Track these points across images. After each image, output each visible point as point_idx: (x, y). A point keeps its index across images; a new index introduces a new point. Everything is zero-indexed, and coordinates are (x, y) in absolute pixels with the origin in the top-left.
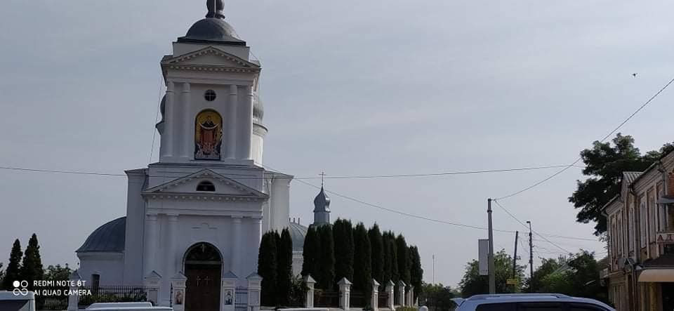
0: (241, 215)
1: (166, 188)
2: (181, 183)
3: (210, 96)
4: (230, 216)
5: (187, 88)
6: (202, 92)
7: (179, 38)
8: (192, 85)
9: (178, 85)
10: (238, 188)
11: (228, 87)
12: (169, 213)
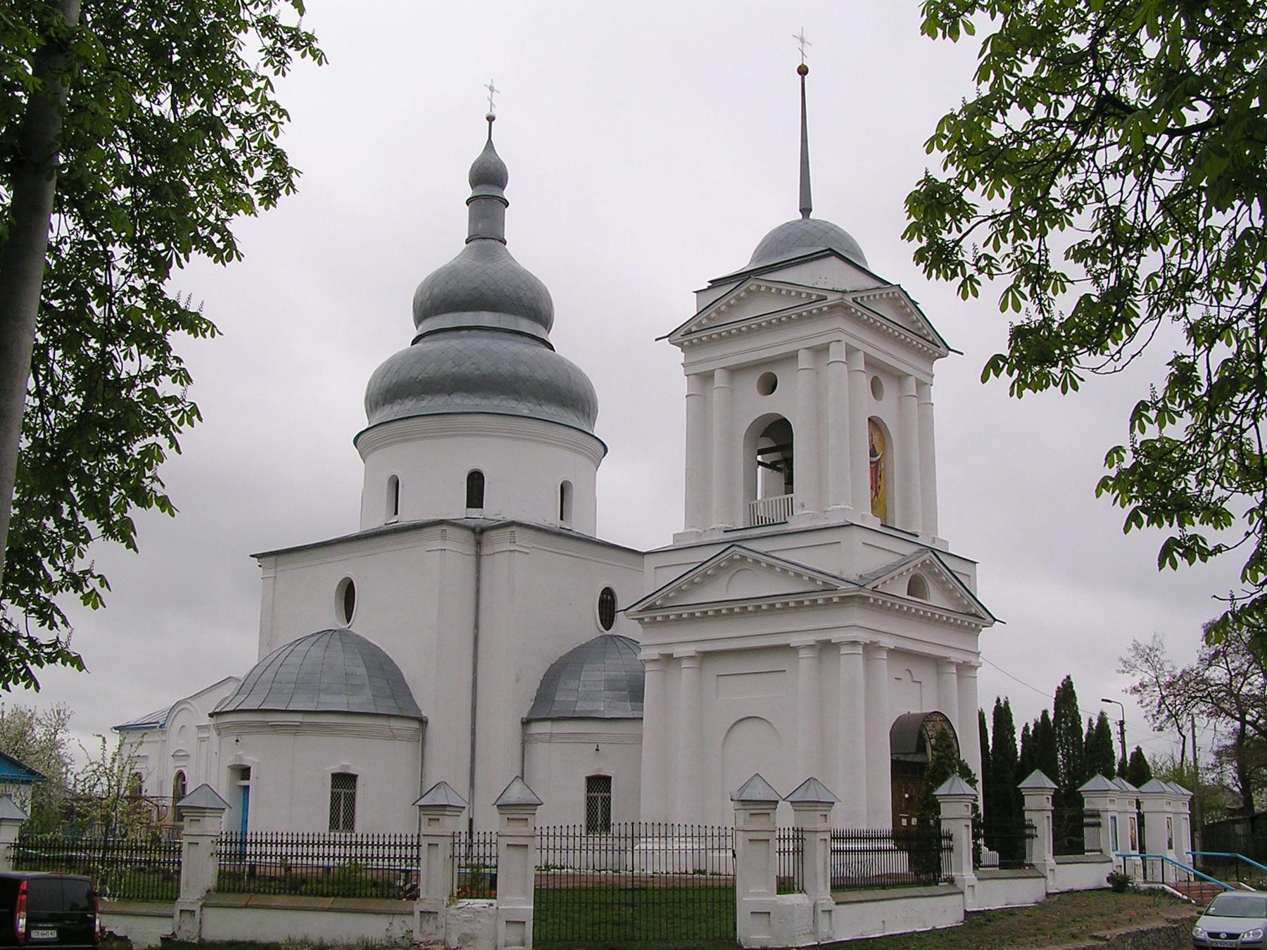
0: (810, 639)
1: (666, 597)
2: (692, 583)
3: (769, 385)
4: (786, 648)
5: (720, 379)
6: (751, 383)
7: (710, 282)
8: (734, 371)
9: (707, 377)
10: (798, 575)
11: (792, 357)
12: (678, 651)
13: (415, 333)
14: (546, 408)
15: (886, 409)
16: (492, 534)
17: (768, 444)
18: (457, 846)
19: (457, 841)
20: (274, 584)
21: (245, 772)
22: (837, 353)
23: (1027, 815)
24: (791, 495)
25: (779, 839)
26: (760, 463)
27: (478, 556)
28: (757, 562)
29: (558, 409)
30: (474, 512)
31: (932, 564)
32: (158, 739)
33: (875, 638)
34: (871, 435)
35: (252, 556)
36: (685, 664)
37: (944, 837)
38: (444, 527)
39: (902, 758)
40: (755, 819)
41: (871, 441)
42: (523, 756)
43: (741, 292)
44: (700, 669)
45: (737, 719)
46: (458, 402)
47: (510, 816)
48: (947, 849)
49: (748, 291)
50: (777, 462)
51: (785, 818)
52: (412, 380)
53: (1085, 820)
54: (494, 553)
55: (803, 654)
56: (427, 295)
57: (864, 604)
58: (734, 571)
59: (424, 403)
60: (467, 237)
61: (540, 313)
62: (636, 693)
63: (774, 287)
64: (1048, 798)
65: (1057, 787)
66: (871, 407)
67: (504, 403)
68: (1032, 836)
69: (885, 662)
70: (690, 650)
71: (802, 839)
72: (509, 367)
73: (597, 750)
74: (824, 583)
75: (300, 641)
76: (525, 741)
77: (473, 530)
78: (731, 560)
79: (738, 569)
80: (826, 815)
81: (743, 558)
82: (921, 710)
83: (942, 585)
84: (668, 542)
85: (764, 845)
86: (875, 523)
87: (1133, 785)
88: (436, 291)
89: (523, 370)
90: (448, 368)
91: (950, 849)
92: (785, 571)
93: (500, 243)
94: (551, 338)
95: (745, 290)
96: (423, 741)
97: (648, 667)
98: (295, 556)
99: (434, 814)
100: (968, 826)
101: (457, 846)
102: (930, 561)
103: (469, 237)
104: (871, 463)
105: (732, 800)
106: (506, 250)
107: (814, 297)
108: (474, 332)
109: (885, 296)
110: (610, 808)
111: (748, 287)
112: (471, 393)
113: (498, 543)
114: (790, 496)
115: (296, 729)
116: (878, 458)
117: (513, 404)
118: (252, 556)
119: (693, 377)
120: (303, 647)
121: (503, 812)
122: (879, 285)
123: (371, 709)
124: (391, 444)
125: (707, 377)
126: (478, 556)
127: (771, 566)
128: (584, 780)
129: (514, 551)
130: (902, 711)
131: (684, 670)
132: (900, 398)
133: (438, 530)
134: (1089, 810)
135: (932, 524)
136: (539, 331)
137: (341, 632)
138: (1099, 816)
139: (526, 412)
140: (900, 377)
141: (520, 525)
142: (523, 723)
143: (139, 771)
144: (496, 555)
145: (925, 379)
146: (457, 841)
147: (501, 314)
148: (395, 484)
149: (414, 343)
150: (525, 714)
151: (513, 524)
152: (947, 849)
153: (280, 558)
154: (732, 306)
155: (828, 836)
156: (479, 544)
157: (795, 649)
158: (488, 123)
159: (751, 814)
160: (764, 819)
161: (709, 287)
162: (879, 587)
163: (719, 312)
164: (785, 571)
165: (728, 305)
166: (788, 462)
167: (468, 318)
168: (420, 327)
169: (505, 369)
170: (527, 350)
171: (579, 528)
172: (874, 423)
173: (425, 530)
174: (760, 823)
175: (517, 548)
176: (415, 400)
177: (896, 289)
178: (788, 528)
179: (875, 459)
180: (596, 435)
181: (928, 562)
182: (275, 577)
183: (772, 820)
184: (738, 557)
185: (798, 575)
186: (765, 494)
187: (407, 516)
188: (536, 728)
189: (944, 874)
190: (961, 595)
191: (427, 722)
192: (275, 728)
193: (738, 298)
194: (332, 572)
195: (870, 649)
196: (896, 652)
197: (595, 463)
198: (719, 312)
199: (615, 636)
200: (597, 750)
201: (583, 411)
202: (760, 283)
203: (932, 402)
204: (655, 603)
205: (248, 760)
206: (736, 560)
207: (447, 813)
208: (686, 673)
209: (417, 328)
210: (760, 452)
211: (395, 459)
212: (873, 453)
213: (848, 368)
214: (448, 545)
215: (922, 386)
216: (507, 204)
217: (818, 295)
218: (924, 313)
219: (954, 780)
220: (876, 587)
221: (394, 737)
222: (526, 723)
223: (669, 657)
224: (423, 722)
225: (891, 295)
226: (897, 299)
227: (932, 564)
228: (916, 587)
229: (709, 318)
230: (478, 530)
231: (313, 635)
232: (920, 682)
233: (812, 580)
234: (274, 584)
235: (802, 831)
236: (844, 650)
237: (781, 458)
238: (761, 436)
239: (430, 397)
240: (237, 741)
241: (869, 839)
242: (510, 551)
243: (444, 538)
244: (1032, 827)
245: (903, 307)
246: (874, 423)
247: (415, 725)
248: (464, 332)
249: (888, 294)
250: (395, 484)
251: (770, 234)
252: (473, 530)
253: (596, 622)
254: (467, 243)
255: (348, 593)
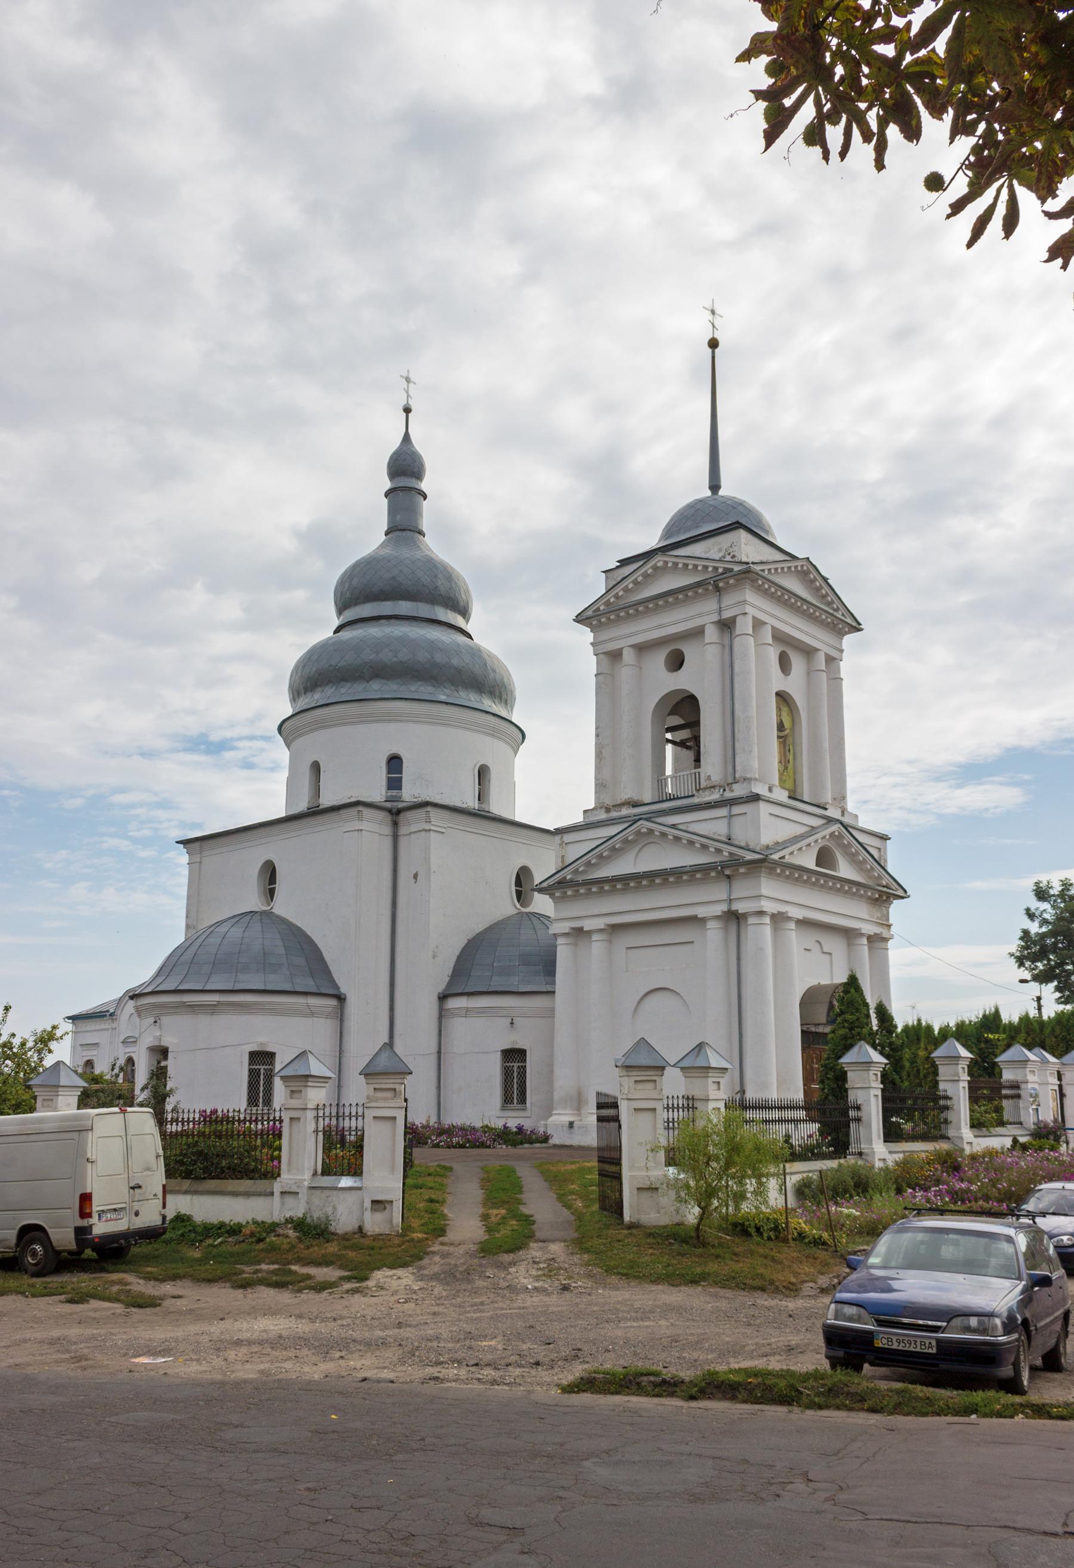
0: (720, 909)
3: (676, 662)
4: (693, 919)
5: (628, 656)
6: (658, 660)
7: (618, 562)
8: (641, 649)
9: (615, 656)
10: (704, 847)
11: (698, 633)
12: (588, 925)
13: (336, 623)
14: (463, 694)
15: (794, 684)
16: (409, 815)
17: (676, 721)
18: (321, 1119)
19: (321, 1113)
20: (200, 870)
21: (164, 1052)
22: (744, 625)
23: (942, 1086)
24: (699, 770)
25: (668, 1108)
26: (668, 741)
27: (395, 837)
28: (664, 835)
29: (475, 696)
30: (394, 793)
31: (841, 836)
32: (106, 1026)
33: (783, 908)
34: (779, 709)
35: (177, 842)
36: (595, 937)
37: (852, 1108)
38: (360, 808)
39: (813, 1029)
40: (640, 1086)
41: (779, 715)
42: (440, 1031)
43: (648, 568)
44: (611, 942)
45: (648, 990)
46: (375, 687)
47: (377, 1086)
48: (855, 1120)
49: (655, 568)
50: (687, 740)
51: (674, 1084)
52: (331, 668)
53: (1004, 1092)
54: (411, 833)
55: (711, 924)
56: (347, 585)
57: (770, 874)
58: (642, 844)
59: (343, 690)
60: (386, 529)
61: (458, 602)
62: (549, 968)
63: (681, 561)
64: (963, 1068)
65: (972, 1056)
66: (778, 682)
67: (422, 688)
68: (947, 1108)
69: (794, 932)
70: (600, 923)
71: (693, 1108)
72: (426, 654)
73: (512, 1023)
74: (731, 854)
75: (219, 923)
76: (442, 1015)
77: (390, 811)
78: (638, 833)
79: (648, 841)
80: (719, 1083)
81: (651, 831)
82: (832, 979)
83: (852, 858)
84: (579, 819)
85: (648, 1116)
86: (782, 795)
87: (1054, 1055)
88: (355, 582)
89: (439, 658)
90: (368, 656)
91: (858, 1120)
92: (691, 843)
93: (418, 535)
94: (469, 628)
95: (651, 567)
96: (341, 1017)
97: (560, 941)
98: (221, 840)
99: (295, 1085)
100: (877, 1096)
101: (321, 1119)
102: (839, 833)
103: (388, 529)
104: (779, 737)
105: (617, 1066)
106: (424, 541)
107: (720, 570)
108: (393, 621)
109: (793, 569)
110: (525, 1081)
111: (656, 564)
112: (389, 679)
113: (412, 822)
114: (697, 770)
115: (213, 1009)
116: (786, 732)
117: (430, 689)
118: (177, 842)
119: (602, 656)
120: (223, 929)
121: (370, 1081)
122: (788, 558)
123: (288, 987)
124: (312, 731)
125: (615, 656)
126: (395, 837)
127: (677, 839)
128: (499, 1054)
129: (429, 830)
130: (814, 982)
131: (594, 943)
132: (808, 673)
133: (353, 811)
134: (1008, 1081)
135: (841, 799)
136: (460, 621)
137: (263, 913)
138: (1018, 1087)
139: (443, 698)
140: (808, 652)
141: (436, 805)
142: (439, 998)
143: (90, 1058)
144: (413, 836)
145: (833, 653)
146: (321, 1113)
147: (420, 604)
148: (316, 767)
149: (336, 631)
150: (441, 987)
151: (427, 804)
152: (855, 1120)
153: (205, 844)
154: (638, 583)
155: (722, 1105)
156: (395, 824)
157: (702, 921)
158: (404, 414)
159: (636, 1081)
160: (650, 1086)
161: (617, 567)
162: (787, 857)
163: (626, 590)
164: (691, 843)
165: (636, 583)
166: (696, 738)
167: (386, 608)
168: (341, 618)
169: (423, 656)
170: (444, 638)
171: (496, 807)
172: (783, 697)
173: (342, 812)
174: (647, 1091)
175: (433, 828)
176: (334, 688)
177: (804, 563)
178: (695, 800)
179: (782, 734)
180: (513, 720)
181: (837, 833)
182: (200, 862)
183: (658, 1087)
184: (645, 830)
185: (704, 847)
186: (676, 769)
187: (327, 800)
188: (453, 1003)
189: (853, 1148)
190: (872, 868)
191: (345, 999)
192: (193, 1008)
193: (646, 576)
194: (255, 855)
195: (778, 919)
196: (805, 924)
197: (512, 747)
198: (626, 590)
199: (531, 913)
200: (512, 1023)
201: (500, 697)
202: (666, 559)
203: (842, 676)
204: (565, 877)
205: (167, 1041)
206: (644, 833)
207: (310, 1084)
208: (597, 946)
209: (339, 619)
210: (669, 730)
211: (316, 745)
212: (781, 727)
213: (755, 641)
214: (364, 825)
215: (832, 660)
216: (425, 497)
217: (724, 568)
218: (834, 587)
219: (861, 1047)
220: (783, 857)
221: (312, 1014)
222: (443, 998)
223: (580, 930)
224: (341, 998)
225: (799, 568)
226: (806, 573)
227: (841, 836)
228: (824, 857)
229: (617, 597)
230: (394, 811)
231: (234, 917)
232: (830, 954)
233: (719, 851)
234: (200, 870)
235: (693, 1099)
236: (751, 920)
237: (690, 736)
238: (669, 714)
239: (349, 685)
240: (155, 1022)
241: (769, 1108)
242: (426, 830)
243: (360, 819)
244: (947, 1098)
245: (813, 581)
246: (783, 697)
247: (333, 1002)
248: (383, 621)
249: (796, 567)
250: (316, 767)
251: (679, 512)
252: (390, 811)
253: (513, 900)
254: (386, 535)
255: (270, 874)
